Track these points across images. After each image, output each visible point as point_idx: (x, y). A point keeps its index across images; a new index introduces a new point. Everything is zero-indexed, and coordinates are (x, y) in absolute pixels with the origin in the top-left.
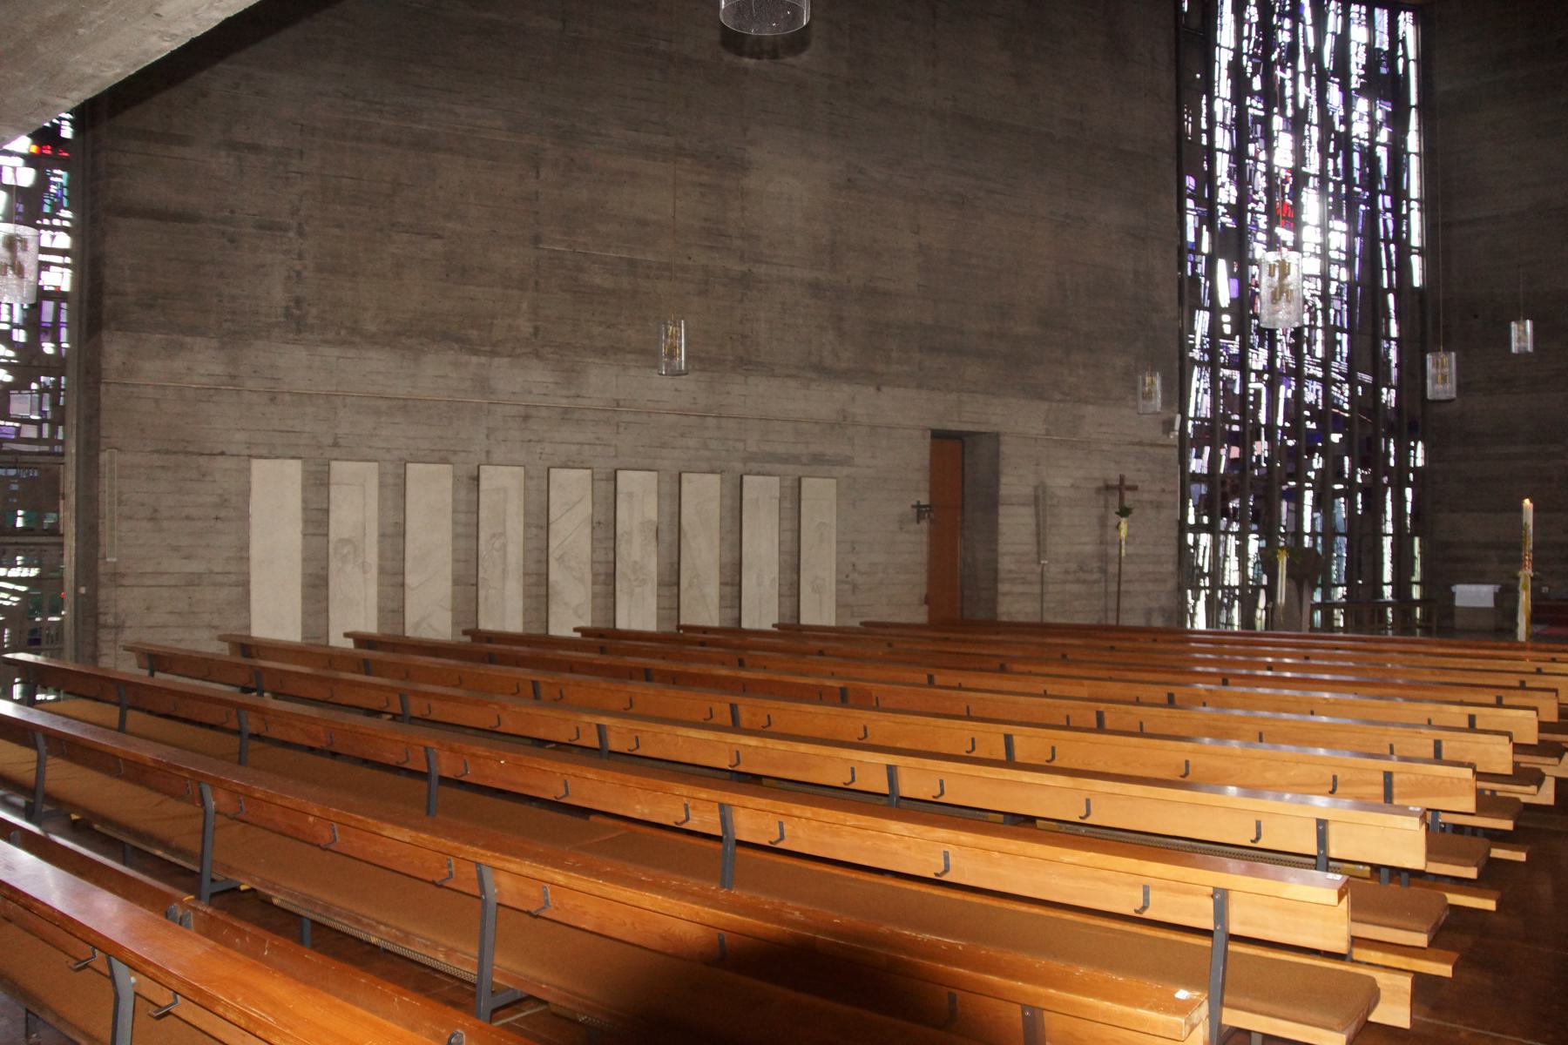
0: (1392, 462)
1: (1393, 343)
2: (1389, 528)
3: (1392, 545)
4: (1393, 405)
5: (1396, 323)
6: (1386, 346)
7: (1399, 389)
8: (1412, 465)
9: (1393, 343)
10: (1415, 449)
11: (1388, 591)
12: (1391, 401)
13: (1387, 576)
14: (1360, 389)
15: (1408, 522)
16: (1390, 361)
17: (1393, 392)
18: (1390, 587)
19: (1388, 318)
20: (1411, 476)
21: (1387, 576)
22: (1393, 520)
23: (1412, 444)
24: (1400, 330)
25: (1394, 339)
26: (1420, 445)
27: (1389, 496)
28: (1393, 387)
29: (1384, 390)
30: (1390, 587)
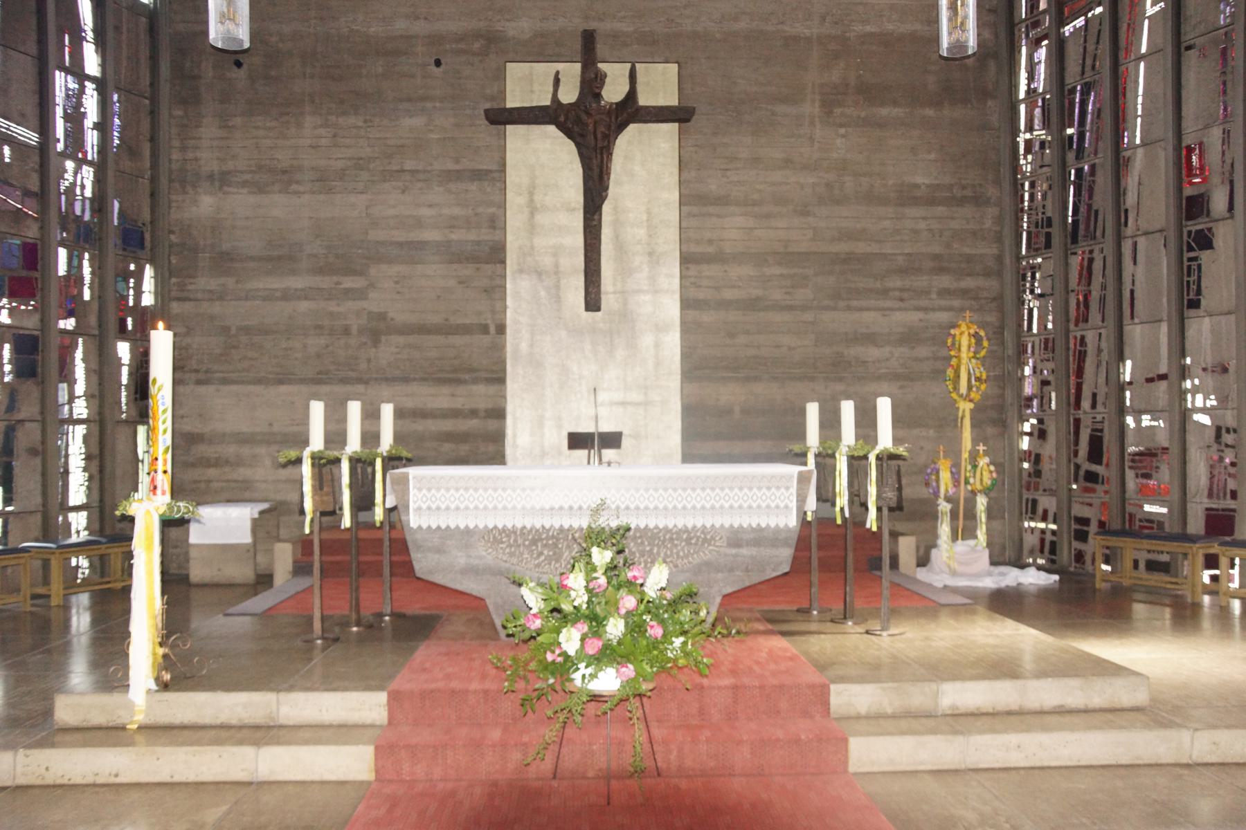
0: (87, 295)
1: (90, 87)
2: (81, 409)
3: (86, 439)
4: (88, 193)
5: (97, 51)
6: (73, 85)
7: (100, 168)
8: (131, 303)
9: (90, 87)
10: (139, 276)
11: (79, 521)
12: (83, 187)
13: (77, 492)
14: (7, 151)
15: (124, 400)
16: (84, 115)
17: (88, 173)
18: (83, 515)
19: (78, 40)
20: (130, 321)
21: (77, 492)
22: (88, 396)
23: (132, 267)
24: (103, 65)
25: (92, 79)
26: (149, 271)
27: (79, 354)
28: (90, 163)
29: (70, 165)
30: (83, 515)
